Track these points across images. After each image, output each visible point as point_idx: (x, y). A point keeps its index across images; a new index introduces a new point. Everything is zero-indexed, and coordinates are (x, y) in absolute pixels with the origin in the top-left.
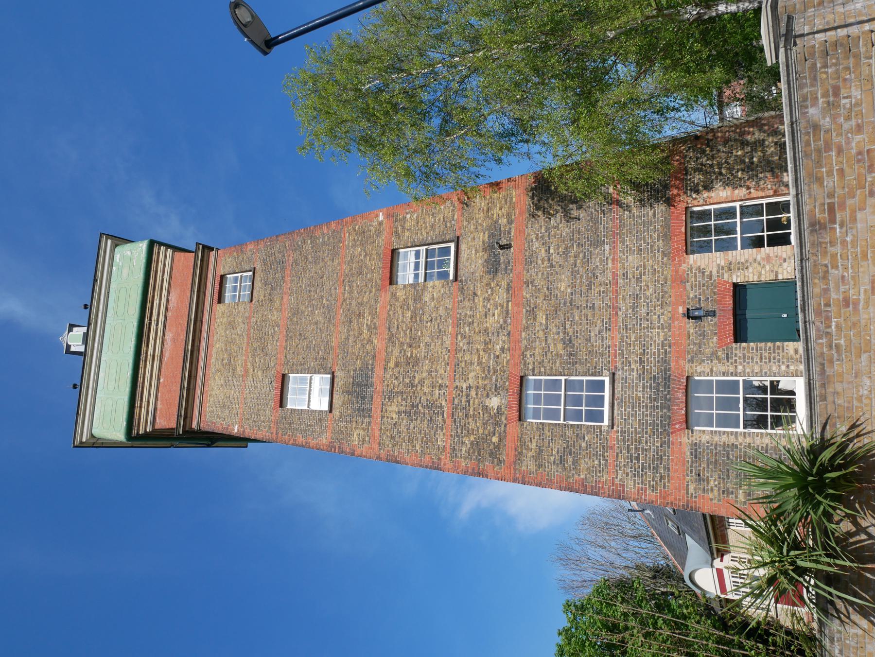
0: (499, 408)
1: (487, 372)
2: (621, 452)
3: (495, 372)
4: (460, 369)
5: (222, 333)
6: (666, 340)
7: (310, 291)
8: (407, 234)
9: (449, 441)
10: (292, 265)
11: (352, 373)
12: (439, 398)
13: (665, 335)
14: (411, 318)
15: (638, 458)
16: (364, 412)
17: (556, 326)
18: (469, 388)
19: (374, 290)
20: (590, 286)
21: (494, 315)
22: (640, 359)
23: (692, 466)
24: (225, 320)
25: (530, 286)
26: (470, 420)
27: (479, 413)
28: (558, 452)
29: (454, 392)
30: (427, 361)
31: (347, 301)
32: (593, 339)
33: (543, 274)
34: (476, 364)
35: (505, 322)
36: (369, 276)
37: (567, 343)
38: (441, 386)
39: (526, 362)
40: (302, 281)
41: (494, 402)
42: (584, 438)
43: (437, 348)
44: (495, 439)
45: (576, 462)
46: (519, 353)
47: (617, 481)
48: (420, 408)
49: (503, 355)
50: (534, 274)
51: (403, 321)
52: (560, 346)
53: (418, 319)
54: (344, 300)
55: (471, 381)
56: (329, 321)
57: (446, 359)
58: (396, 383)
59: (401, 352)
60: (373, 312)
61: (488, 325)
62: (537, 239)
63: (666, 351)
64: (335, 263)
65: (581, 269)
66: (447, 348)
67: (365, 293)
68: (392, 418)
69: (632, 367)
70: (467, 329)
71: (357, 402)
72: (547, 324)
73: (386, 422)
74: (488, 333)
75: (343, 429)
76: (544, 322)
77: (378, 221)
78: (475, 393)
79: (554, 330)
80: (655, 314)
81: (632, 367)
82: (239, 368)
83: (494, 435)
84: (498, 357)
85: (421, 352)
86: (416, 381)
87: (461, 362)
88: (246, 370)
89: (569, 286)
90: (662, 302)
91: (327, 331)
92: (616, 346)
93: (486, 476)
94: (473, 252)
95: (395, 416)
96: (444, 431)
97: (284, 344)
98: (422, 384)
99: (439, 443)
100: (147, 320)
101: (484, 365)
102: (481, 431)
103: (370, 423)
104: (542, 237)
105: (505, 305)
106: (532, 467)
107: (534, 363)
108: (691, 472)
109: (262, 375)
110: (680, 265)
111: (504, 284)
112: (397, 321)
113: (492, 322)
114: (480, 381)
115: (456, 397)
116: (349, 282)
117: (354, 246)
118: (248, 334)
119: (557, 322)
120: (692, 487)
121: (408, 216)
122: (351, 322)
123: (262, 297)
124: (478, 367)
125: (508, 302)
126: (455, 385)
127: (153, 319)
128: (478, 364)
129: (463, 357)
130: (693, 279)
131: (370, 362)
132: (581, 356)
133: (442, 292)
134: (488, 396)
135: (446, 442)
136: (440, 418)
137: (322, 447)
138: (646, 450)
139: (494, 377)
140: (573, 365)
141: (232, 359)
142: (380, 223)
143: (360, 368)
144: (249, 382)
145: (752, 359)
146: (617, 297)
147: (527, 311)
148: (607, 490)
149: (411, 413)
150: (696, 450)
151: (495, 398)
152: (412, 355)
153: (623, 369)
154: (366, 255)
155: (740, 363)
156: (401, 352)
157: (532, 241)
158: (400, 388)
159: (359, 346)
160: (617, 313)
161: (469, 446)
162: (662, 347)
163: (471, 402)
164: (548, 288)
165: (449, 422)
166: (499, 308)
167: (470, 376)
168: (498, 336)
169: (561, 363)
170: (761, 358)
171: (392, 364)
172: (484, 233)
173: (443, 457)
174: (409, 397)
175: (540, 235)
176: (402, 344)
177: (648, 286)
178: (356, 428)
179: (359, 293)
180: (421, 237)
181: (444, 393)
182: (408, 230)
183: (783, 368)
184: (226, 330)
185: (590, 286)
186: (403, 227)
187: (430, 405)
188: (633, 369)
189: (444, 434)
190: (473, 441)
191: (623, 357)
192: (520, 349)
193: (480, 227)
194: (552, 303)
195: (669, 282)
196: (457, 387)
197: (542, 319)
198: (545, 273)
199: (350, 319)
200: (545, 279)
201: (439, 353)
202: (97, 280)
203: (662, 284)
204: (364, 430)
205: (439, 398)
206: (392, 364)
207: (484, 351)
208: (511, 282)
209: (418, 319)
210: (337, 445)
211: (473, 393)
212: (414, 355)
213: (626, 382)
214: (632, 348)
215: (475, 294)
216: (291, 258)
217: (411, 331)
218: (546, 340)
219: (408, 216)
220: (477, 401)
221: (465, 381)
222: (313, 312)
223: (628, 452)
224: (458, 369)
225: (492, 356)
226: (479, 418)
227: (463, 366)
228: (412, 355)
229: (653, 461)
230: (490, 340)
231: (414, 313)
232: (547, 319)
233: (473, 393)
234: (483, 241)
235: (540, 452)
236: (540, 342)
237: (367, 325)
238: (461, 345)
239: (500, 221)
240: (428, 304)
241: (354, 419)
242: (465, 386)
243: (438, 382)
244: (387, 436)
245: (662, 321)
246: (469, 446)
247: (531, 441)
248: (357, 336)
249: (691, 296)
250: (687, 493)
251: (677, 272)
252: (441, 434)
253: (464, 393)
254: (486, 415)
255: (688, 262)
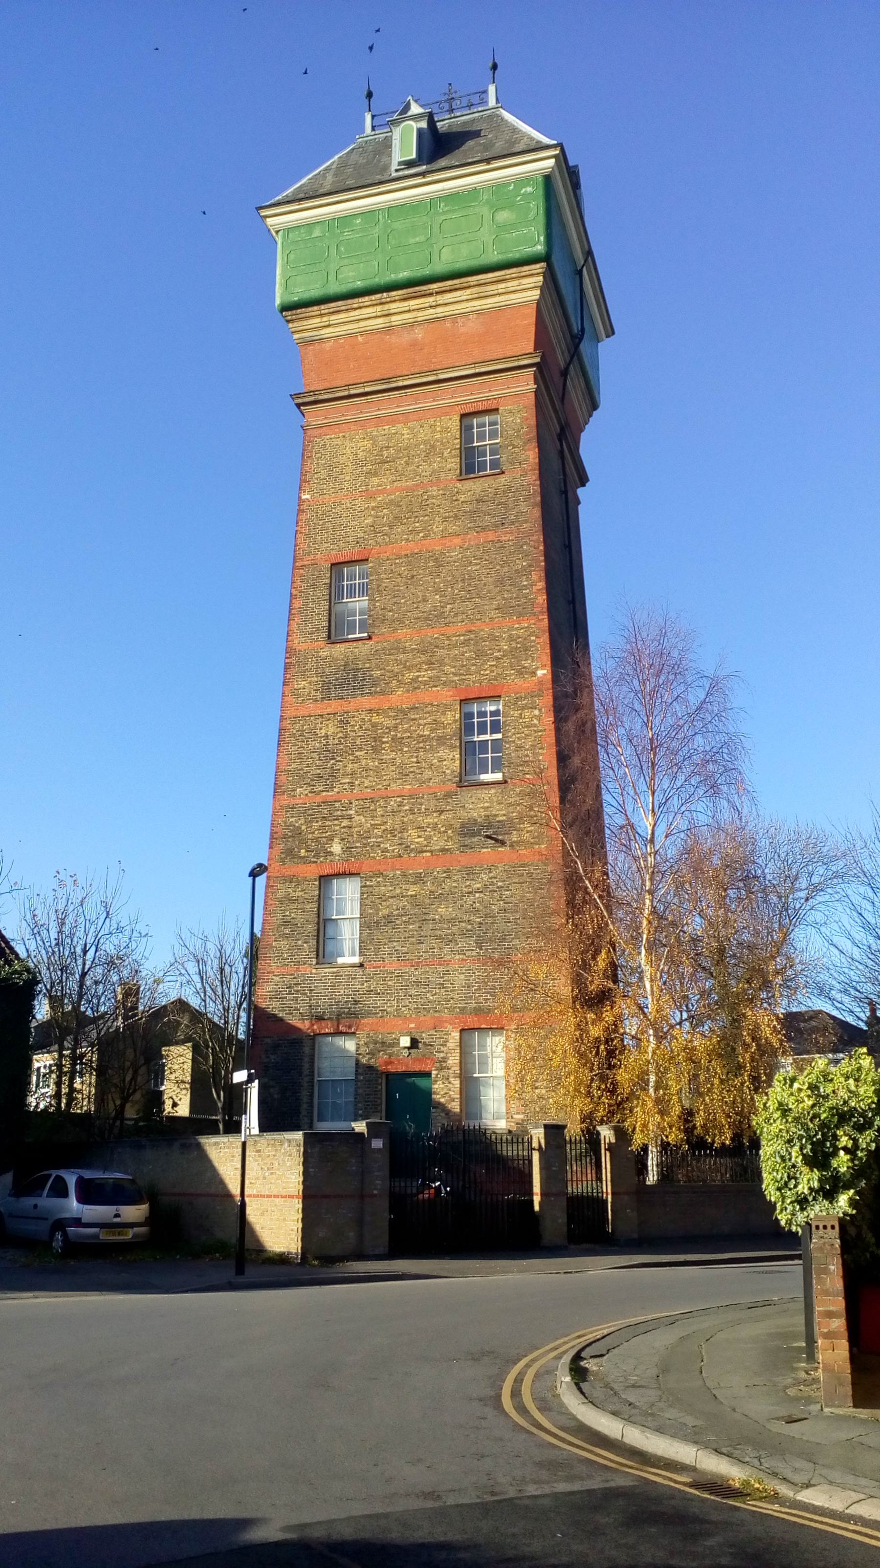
0: (331, 854)
1: (364, 836)
2: (294, 978)
3: (365, 846)
4: (368, 806)
5: (422, 436)
6: (387, 1013)
7: (463, 580)
8: (517, 713)
9: (301, 801)
10: (499, 541)
11: (367, 665)
12: (341, 784)
13: (391, 1013)
14: (422, 736)
15: (290, 993)
16: (327, 690)
17: (405, 906)
18: (350, 818)
19: (456, 678)
20: (439, 937)
21: (419, 837)
22: (372, 991)
23: (285, 1040)
24: (438, 436)
25: (445, 875)
26: (320, 823)
27: (327, 832)
28: (293, 918)
29: (346, 801)
30: (376, 764)
31: (447, 642)
32: (391, 945)
33: (456, 887)
34: (373, 822)
35: (412, 850)
36: (473, 668)
37: (389, 920)
38: (351, 784)
39: (373, 877)
40: (476, 564)
41: (336, 848)
42: (306, 943)
43: (391, 772)
44: (303, 852)
45: (285, 937)
46: (382, 868)
47: (271, 976)
48: (332, 762)
49: (380, 851)
50: (456, 878)
51: (419, 725)
52: (386, 912)
53: (421, 745)
54: (448, 638)
55: (357, 818)
56: (427, 619)
57: (378, 787)
58: (356, 728)
59: (387, 728)
60: (434, 682)
61: (410, 832)
62: (491, 878)
63: (378, 1013)
64: (493, 614)
65: (456, 928)
66: (389, 785)
67: (454, 667)
68: (321, 729)
69: (365, 984)
70: (407, 808)
71: (337, 679)
72: (408, 896)
73: (318, 721)
74: (401, 832)
75: (309, 665)
76: (409, 893)
77: (537, 668)
78: (345, 825)
79: (401, 905)
80: (410, 1002)
81: (365, 984)
82: (375, 480)
83: (307, 851)
84: (379, 846)
85: (388, 755)
86: (357, 753)
87: (375, 804)
88: (371, 496)
89: (442, 917)
90: (420, 1008)
91: (415, 619)
92: (384, 967)
93: (271, 847)
94: (486, 805)
95: (324, 732)
96: (309, 795)
97: (403, 553)
98: (357, 760)
99: (298, 790)
100: (435, 286)
101: (371, 832)
102: (310, 836)
103: (316, 701)
104: (492, 884)
105: (428, 848)
106: (280, 894)
107: (371, 886)
108: (280, 1040)
109: (367, 525)
110: (451, 1024)
111: (450, 845)
112: (420, 718)
113: (414, 837)
114: (356, 829)
115: (341, 804)
116: (469, 639)
117: (511, 639)
118: (417, 485)
119: (409, 906)
120: (268, 1040)
121: (536, 712)
122: (424, 652)
123: (462, 498)
124: (369, 825)
125: (431, 851)
126: (353, 801)
127: (439, 297)
128: (372, 825)
129: (381, 807)
130: (438, 1036)
131: (378, 689)
132: (377, 935)
133: (448, 771)
134: (343, 839)
135: (301, 799)
136: (321, 788)
137: (290, 638)
138: (297, 1000)
139: (358, 845)
140: (368, 927)
141: (386, 466)
142: (534, 673)
143: (372, 675)
144: (360, 503)
145: (368, 1088)
146: (427, 965)
147: (420, 874)
148: (263, 967)
149: (329, 753)
150: (297, 1043)
151: (340, 849)
152: (384, 743)
153: (364, 975)
154: (498, 658)
155: (364, 1078)
156: (387, 728)
157: (489, 872)
158: (351, 733)
159: (396, 669)
160: (413, 966)
161: (297, 825)
162: (381, 1010)
163: (336, 822)
164: (441, 894)
165: (318, 799)
166: (425, 842)
167: (361, 817)
168: (399, 844)
169: (371, 914)
170: (368, 1095)
171: (375, 719)
172: (504, 815)
173: (285, 797)
174: (342, 747)
175: (495, 880)
176: (396, 727)
177: (435, 994)
178: (310, 683)
179: (455, 658)
180: (510, 734)
181: (346, 789)
182: (521, 714)
183: (360, 1112)
184: (425, 442)
185: (439, 937)
186: (523, 708)
187: (333, 775)
188: (363, 985)
189: (307, 795)
190: (301, 828)
191: (373, 974)
192: (385, 870)
193: (511, 809)
194: (427, 901)
195: (437, 1015)
196: (351, 803)
197: (413, 890)
198: (456, 890)
199: (426, 651)
200: (450, 891)
201: (385, 778)
202: (488, 163)
203: (436, 1008)
204: (309, 694)
205: (341, 784)
206: (375, 719)
207: (384, 831)
208: (451, 853)
209: (421, 745)
210: (294, 660)
211: (345, 823)
212: (383, 746)
213: (352, 979)
214: (382, 982)
215: (441, 812)
216: (509, 537)
217: (409, 737)
218: (392, 897)
219: (536, 712)
220: (337, 828)
221: (356, 812)
222: (437, 591)
223: (294, 984)
224: (368, 804)
225: (379, 840)
226: (322, 832)
227: (371, 808)
228: (384, 743)
229: (288, 1007)
230: (395, 836)
231: (428, 738)
232: (412, 896)
233: (345, 823)
234: (496, 815)
235: (293, 901)
236: (391, 890)
237: (418, 676)
238: (392, 803)
239: (515, 832)
240: (435, 755)
241: (319, 679)
242: (352, 812)
243: (356, 780)
244: (303, 726)
245: (403, 1009)
246: (297, 825)
247: (302, 891)
248: (408, 664)
249: (424, 1035)
250: (264, 1037)
251: (446, 1021)
252: (307, 792)
253: (344, 812)
254: (324, 840)
255: (453, 1031)
